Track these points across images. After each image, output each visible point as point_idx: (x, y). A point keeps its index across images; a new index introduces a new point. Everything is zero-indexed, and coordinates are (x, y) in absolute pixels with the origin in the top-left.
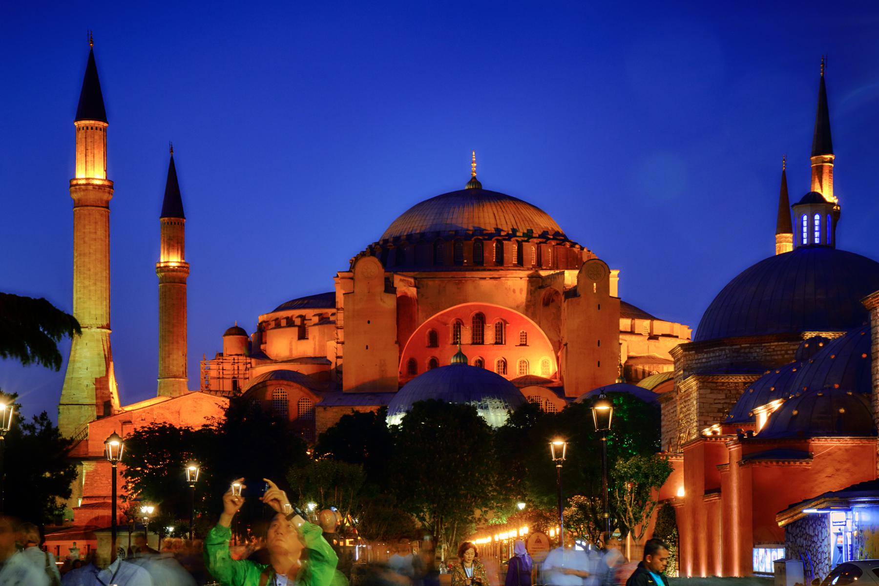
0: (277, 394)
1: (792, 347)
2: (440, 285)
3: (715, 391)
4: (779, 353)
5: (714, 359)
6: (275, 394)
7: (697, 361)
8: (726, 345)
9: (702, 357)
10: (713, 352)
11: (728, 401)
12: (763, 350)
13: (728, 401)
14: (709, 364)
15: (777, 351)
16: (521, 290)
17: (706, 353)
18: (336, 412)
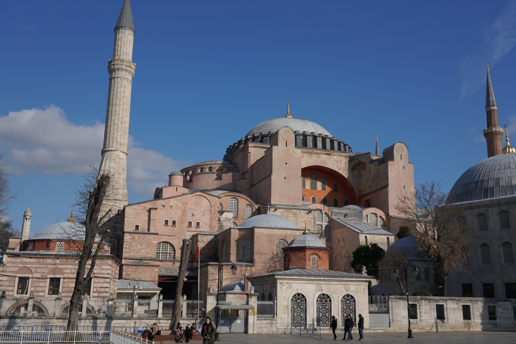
0: (232, 202)
6: (231, 201)
16: (340, 161)
18: (283, 212)
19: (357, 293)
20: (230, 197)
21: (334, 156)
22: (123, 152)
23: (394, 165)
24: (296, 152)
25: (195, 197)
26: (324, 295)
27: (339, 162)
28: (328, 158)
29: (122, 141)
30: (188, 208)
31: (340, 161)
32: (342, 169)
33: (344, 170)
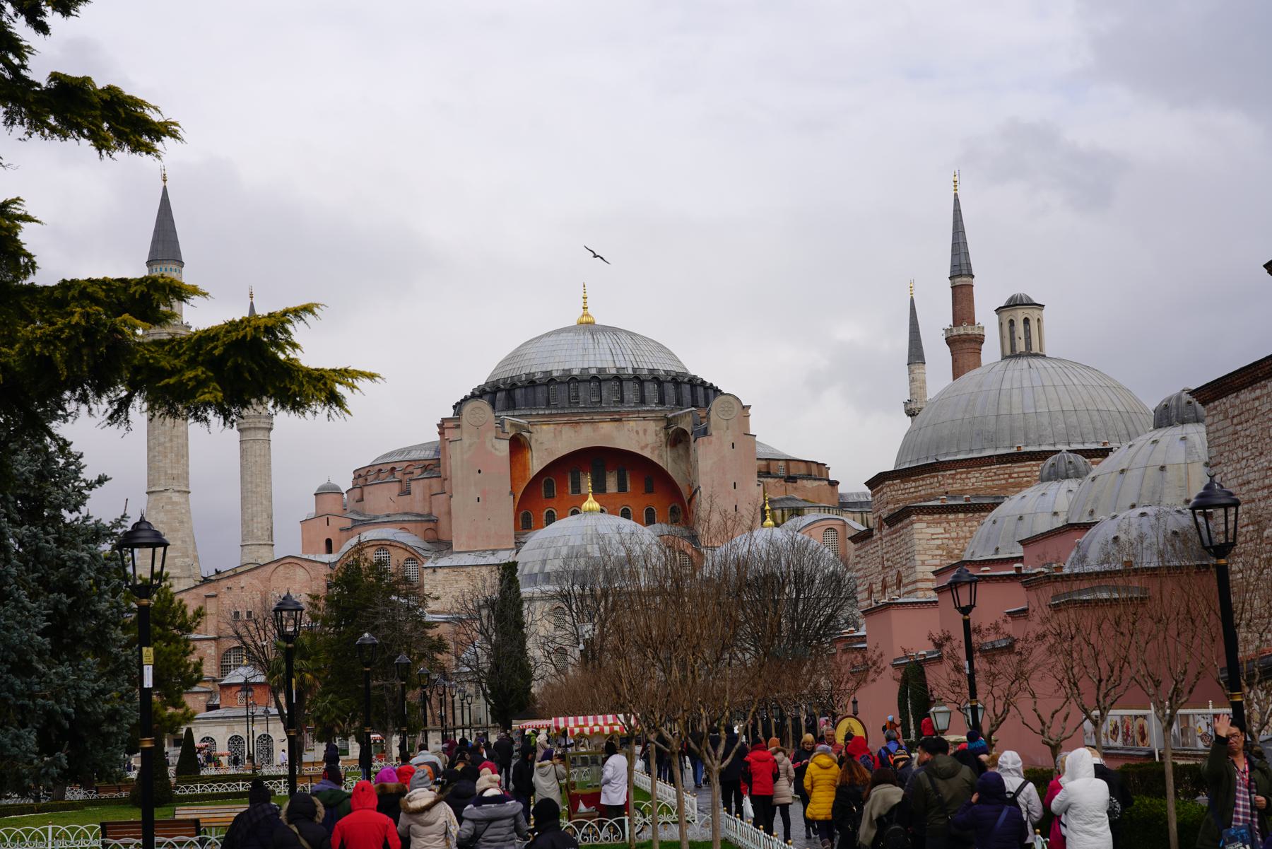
1: (1016, 470)
2: (555, 429)
3: (932, 525)
4: (1002, 477)
5: (924, 487)
7: (903, 492)
8: (939, 471)
9: (909, 486)
10: (923, 479)
11: (947, 535)
12: (983, 475)
13: (947, 535)
14: (918, 494)
15: (999, 475)
16: (645, 431)
17: (914, 481)
19: (275, 732)
20: (375, 548)
21: (631, 422)
22: (179, 491)
23: (710, 443)
24: (497, 446)
25: (281, 568)
26: (236, 736)
27: (641, 433)
28: (616, 428)
29: (175, 472)
30: (272, 587)
31: (645, 431)
32: (649, 447)
33: (653, 449)
